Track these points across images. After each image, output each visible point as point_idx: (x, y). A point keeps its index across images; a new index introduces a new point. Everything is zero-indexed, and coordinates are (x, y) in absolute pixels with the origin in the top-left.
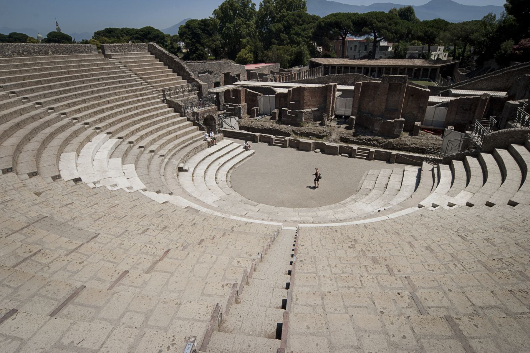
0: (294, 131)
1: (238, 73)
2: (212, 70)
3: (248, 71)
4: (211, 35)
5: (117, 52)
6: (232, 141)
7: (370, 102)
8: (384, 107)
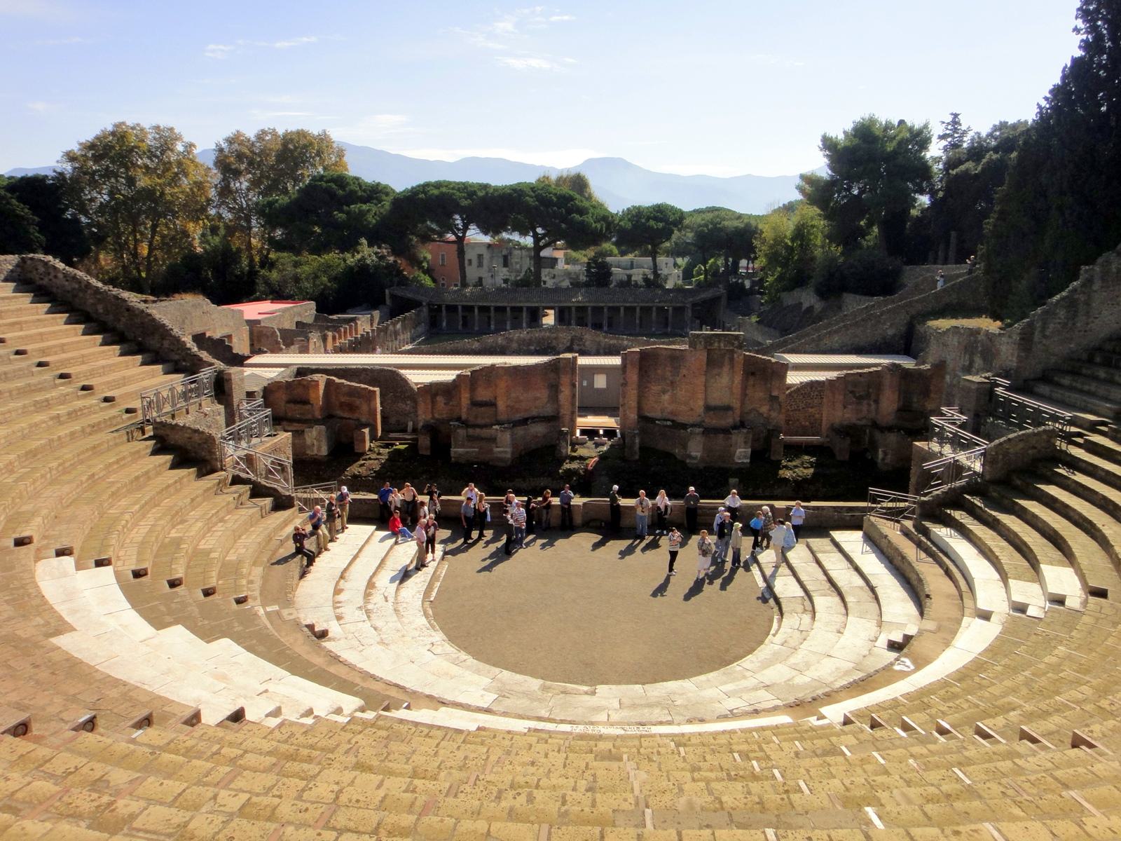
3: (252, 323)
7: (664, 392)
8: (701, 403)
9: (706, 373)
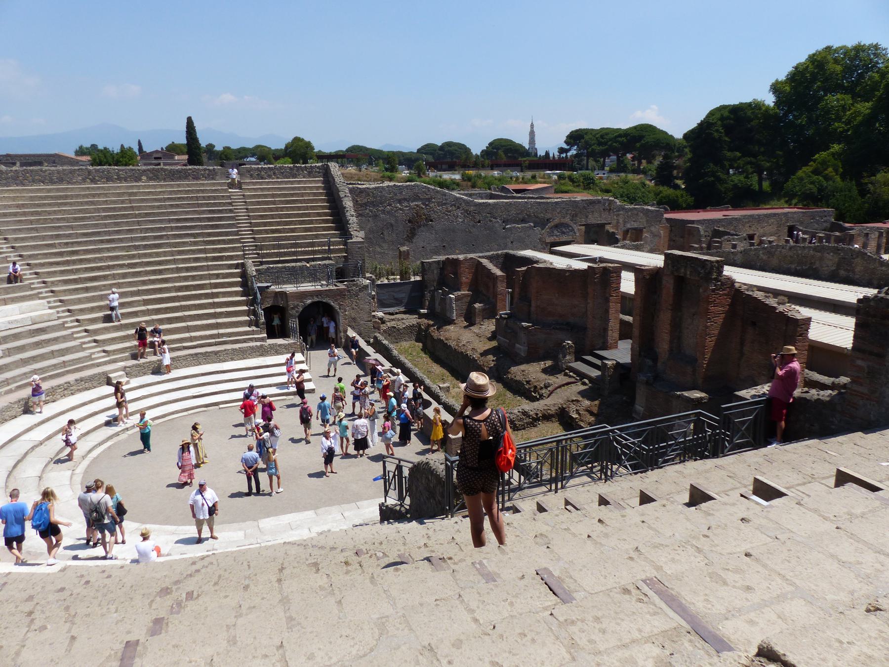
2: (548, 216)
5: (262, 178)
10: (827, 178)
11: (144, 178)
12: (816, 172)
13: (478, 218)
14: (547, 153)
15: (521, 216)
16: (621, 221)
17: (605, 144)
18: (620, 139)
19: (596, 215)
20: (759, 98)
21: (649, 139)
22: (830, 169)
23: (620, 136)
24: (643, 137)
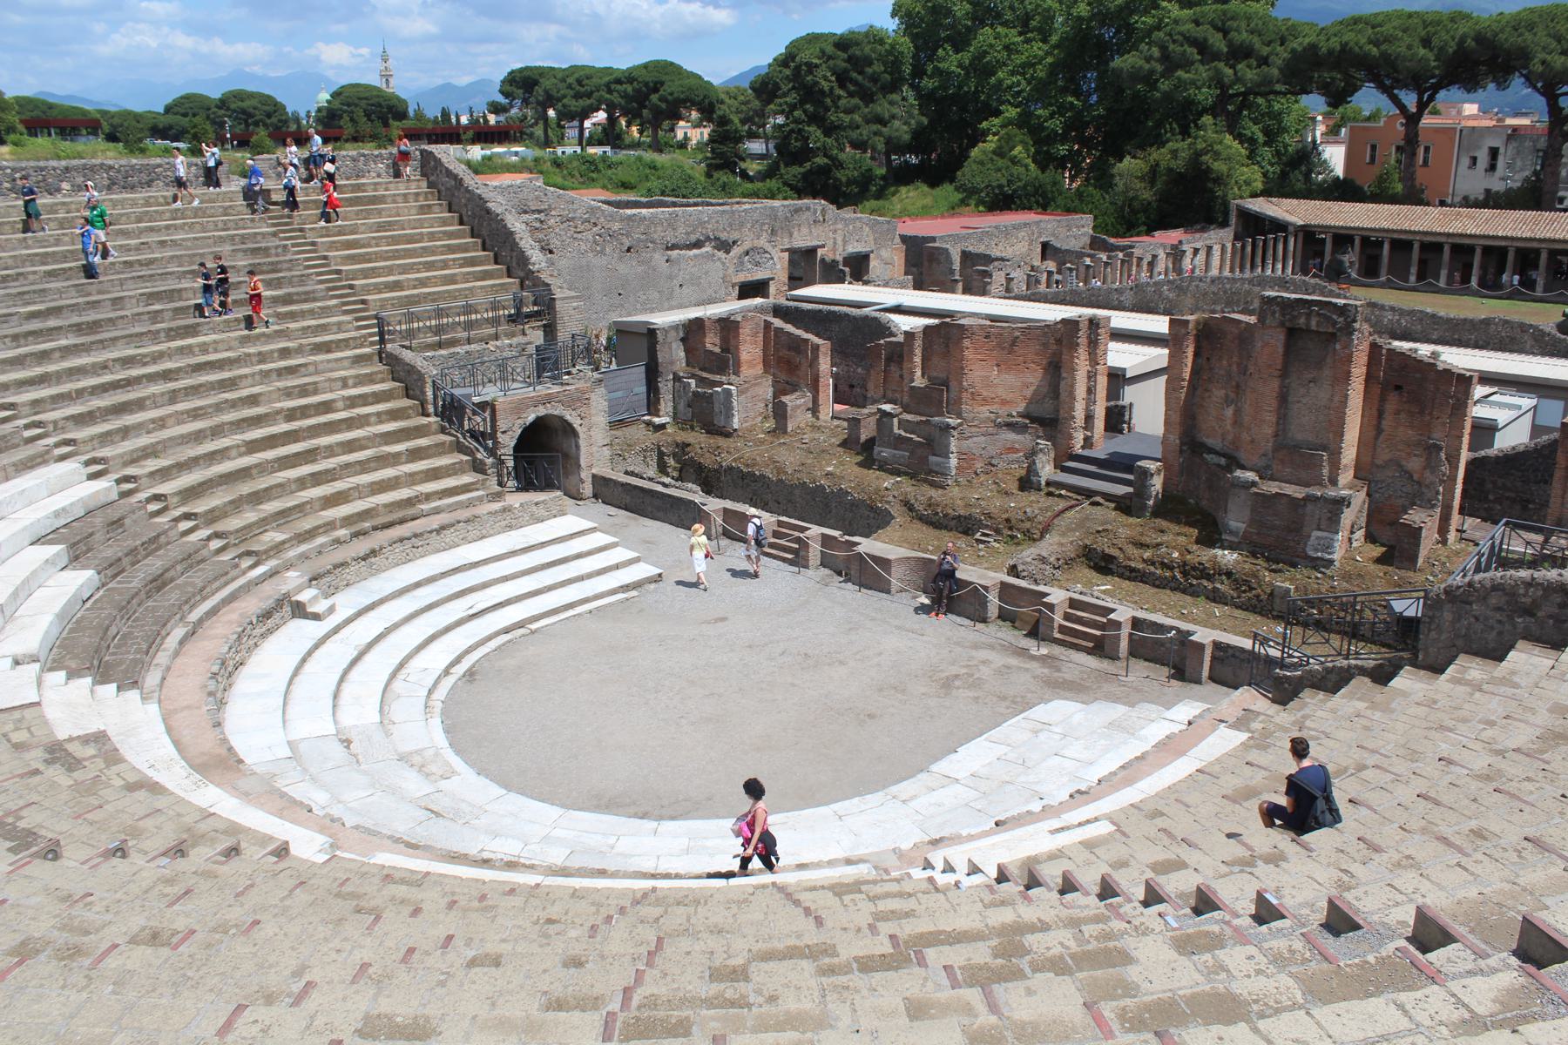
0: (909, 506)
1: (854, 248)
2: (735, 235)
4: (868, 98)
6: (590, 525)
8: (1268, 430)
9: (1284, 373)
10: (1014, 161)
11: (65, 186)
12: (999, 153)
13: (628, 244)
14: (445, 114)
15: (693, 238)
16: (839, 241)
17: (589, 95)
18: (619, 87)
19: (805, 230)
20: (878, 25)
21: (672, 88)
22: (1019, 148)
23: (618, 81)
24: (662, 84)
